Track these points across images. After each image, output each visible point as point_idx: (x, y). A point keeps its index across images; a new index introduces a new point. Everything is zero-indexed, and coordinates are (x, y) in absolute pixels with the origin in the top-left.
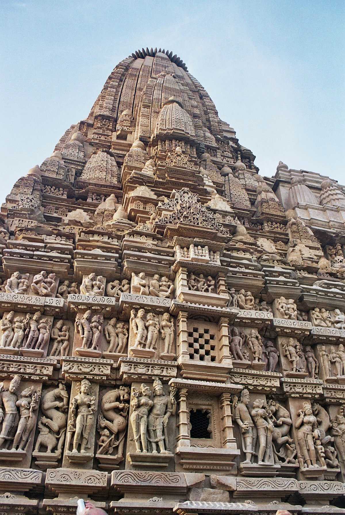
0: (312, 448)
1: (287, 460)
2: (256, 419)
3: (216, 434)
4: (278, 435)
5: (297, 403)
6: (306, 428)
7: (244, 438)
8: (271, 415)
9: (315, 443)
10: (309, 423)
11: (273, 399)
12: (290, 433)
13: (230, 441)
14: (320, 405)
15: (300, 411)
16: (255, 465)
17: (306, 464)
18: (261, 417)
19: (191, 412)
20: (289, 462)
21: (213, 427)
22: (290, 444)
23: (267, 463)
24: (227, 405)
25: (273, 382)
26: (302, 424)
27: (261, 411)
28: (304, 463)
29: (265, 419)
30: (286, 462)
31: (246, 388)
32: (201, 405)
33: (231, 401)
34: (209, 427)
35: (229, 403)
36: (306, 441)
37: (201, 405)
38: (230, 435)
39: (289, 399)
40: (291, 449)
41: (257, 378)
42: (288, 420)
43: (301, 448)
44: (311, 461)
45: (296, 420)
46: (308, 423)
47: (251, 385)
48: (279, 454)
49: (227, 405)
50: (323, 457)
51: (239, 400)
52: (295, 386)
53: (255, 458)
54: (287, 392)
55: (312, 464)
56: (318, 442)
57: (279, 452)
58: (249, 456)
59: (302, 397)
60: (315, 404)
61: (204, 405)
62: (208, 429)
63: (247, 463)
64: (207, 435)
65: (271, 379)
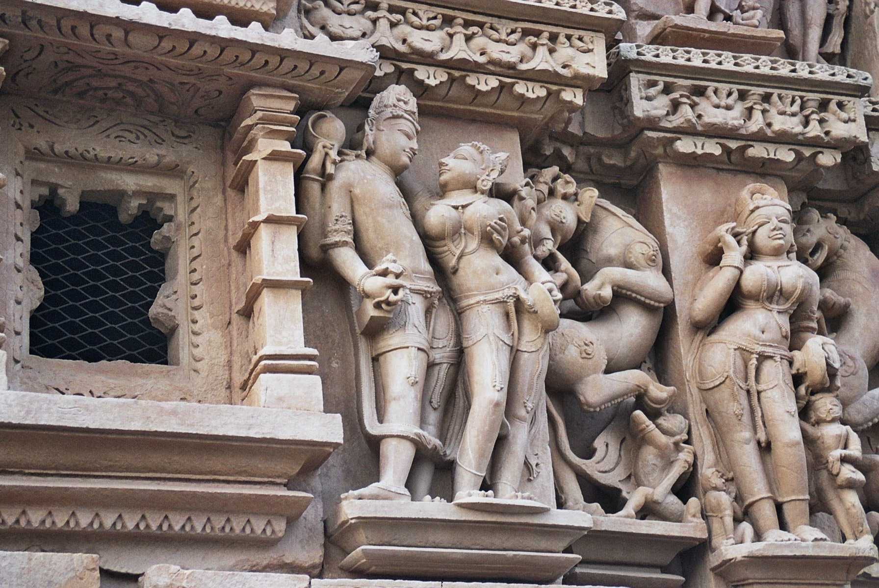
0: (789, 430)
1: (635, 499)
2: (450, 253)
3: (201, 340)
4: (587, 356)
5: (706, 194)
6: (757, 325)
7: (375, 360)
8: (549, 246)
9: (805, 413)
10: (773, 294)
11: (558, 159)
12: (657, 355)
13: (279, 364)
14: (841, 221)
15: (723, 230)
16: (433, 508)
17: (746, 528)
18: (487, 240)
19: (47, 207)
20: (647, 511)
21: (187, 300)
22: (654, 415)
23: (508, 494)
24: (275, 157)
25: (564, 51)
26: (734, 302)
27: (485, 210)
28: (737, 521)
29: (511, 256)
30: (630, 508)
31: (403, 76)
32: (111, 164)
33: (303, 141)
34: (160, 300)
35: (285, 146)
36: (753, 397)
37: (111, 164)
38: (282, 325)
39: (664, 171)
40: (663, 439)
41: (467, 24)
42: (651, 280)
43: (720, 440)
44: (779, 508)
45: (697, 283)
46: (770, 298)
47: (428, 59)
48: (589, 466)
49: (275, 157)
50: (851, 485)
51: (353, 144)
52: (700, 92)
53: (434, 468)
54: (652, 123)
55: (783, 525)
56: (826, 405)
57: (588, 453)
58: (397, 460)
59: (737, 162)
60: (815, 214)
61: (134, 168)
62: (153, 311)
63: (389, 494)
64: (153, 346)
65: (553, 38)
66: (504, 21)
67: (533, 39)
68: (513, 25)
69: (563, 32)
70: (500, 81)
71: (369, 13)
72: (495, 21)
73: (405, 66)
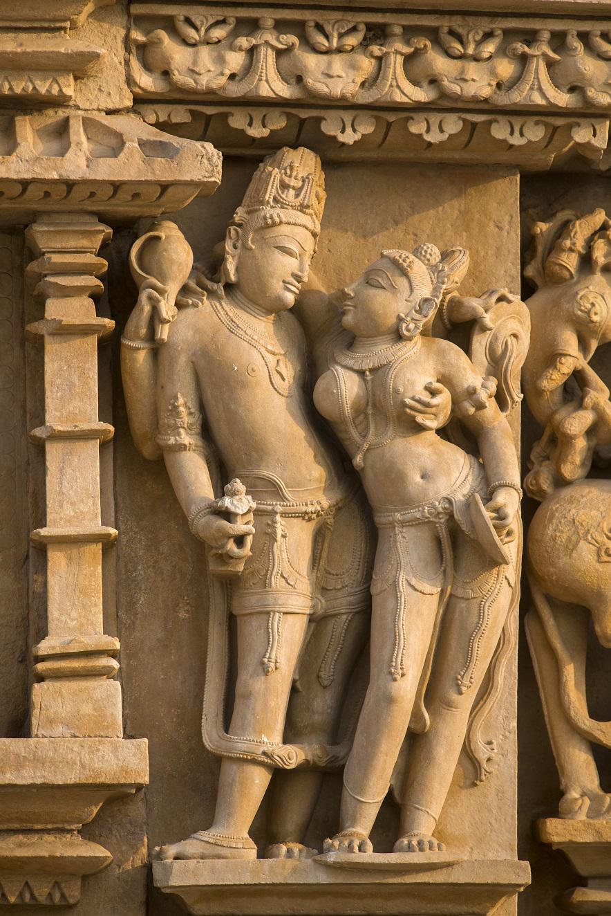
51: (209, 266)
63: (223, 853)
66: (470, 20)
67: (521, 48)
68: (485, 25)
69: (573, 27)
70: (464, 121)
71: (244, 42)
72: (457, 23)
73: (304, 114)
